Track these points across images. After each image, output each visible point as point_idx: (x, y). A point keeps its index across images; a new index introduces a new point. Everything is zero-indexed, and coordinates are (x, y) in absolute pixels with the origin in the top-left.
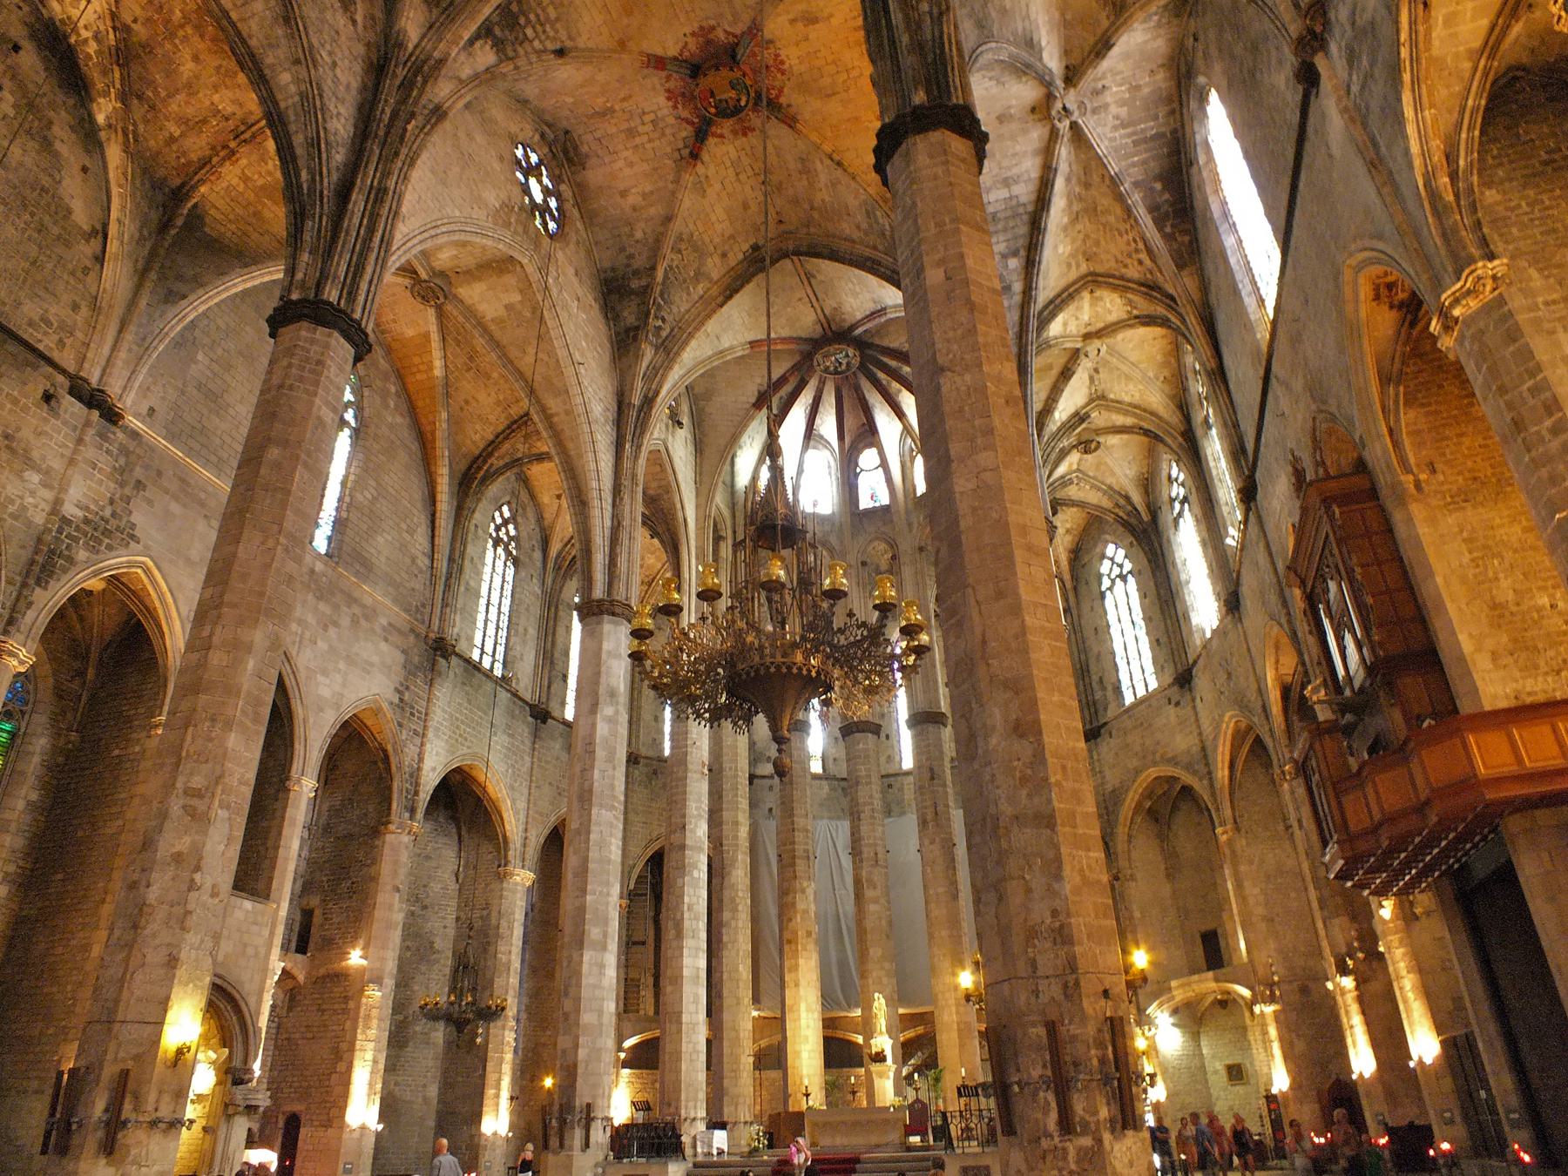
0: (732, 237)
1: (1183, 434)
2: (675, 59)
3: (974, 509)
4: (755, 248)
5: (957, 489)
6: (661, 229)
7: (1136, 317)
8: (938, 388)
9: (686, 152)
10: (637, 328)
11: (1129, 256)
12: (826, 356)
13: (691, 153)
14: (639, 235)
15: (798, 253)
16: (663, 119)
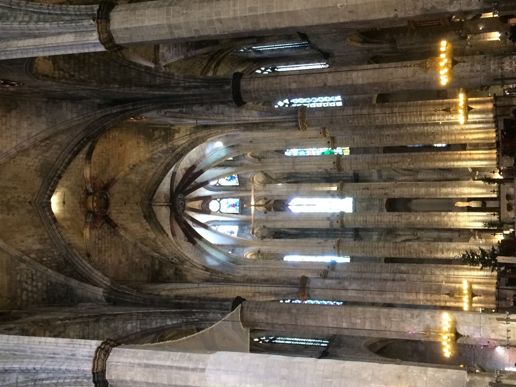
0: (141, 224)
1: (255, 63)
2: (86, 218)
3: (368, 79)
4: (145, 217)
5: (361, 83)
6: (138, 250)
7: (215, 68)
8: (330, 87)
9: (112, 230)
10: (176, 269)
11: (201, 62)
12: (179, 208)
13: (114, 227)
14: (137, 260)
15: (151, 199)
16: (99, 235)
